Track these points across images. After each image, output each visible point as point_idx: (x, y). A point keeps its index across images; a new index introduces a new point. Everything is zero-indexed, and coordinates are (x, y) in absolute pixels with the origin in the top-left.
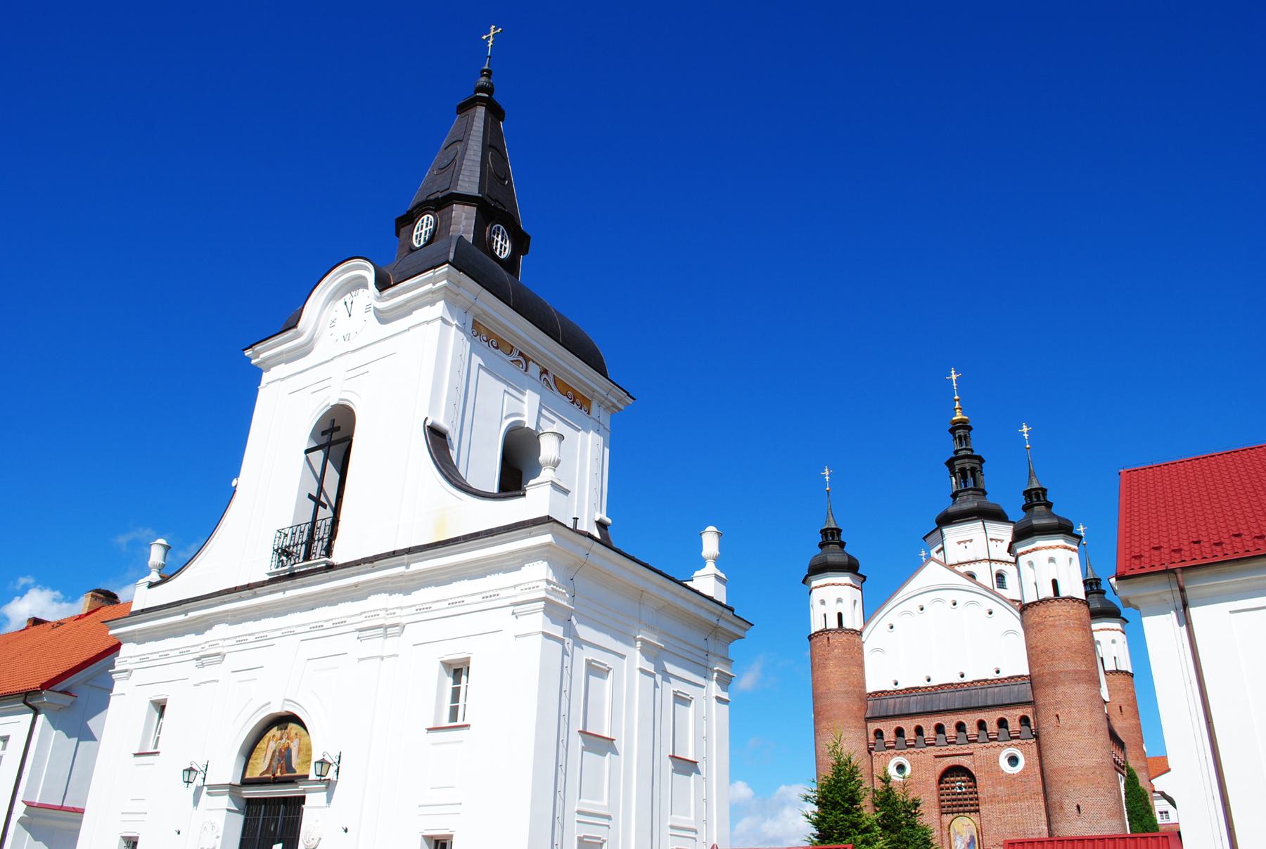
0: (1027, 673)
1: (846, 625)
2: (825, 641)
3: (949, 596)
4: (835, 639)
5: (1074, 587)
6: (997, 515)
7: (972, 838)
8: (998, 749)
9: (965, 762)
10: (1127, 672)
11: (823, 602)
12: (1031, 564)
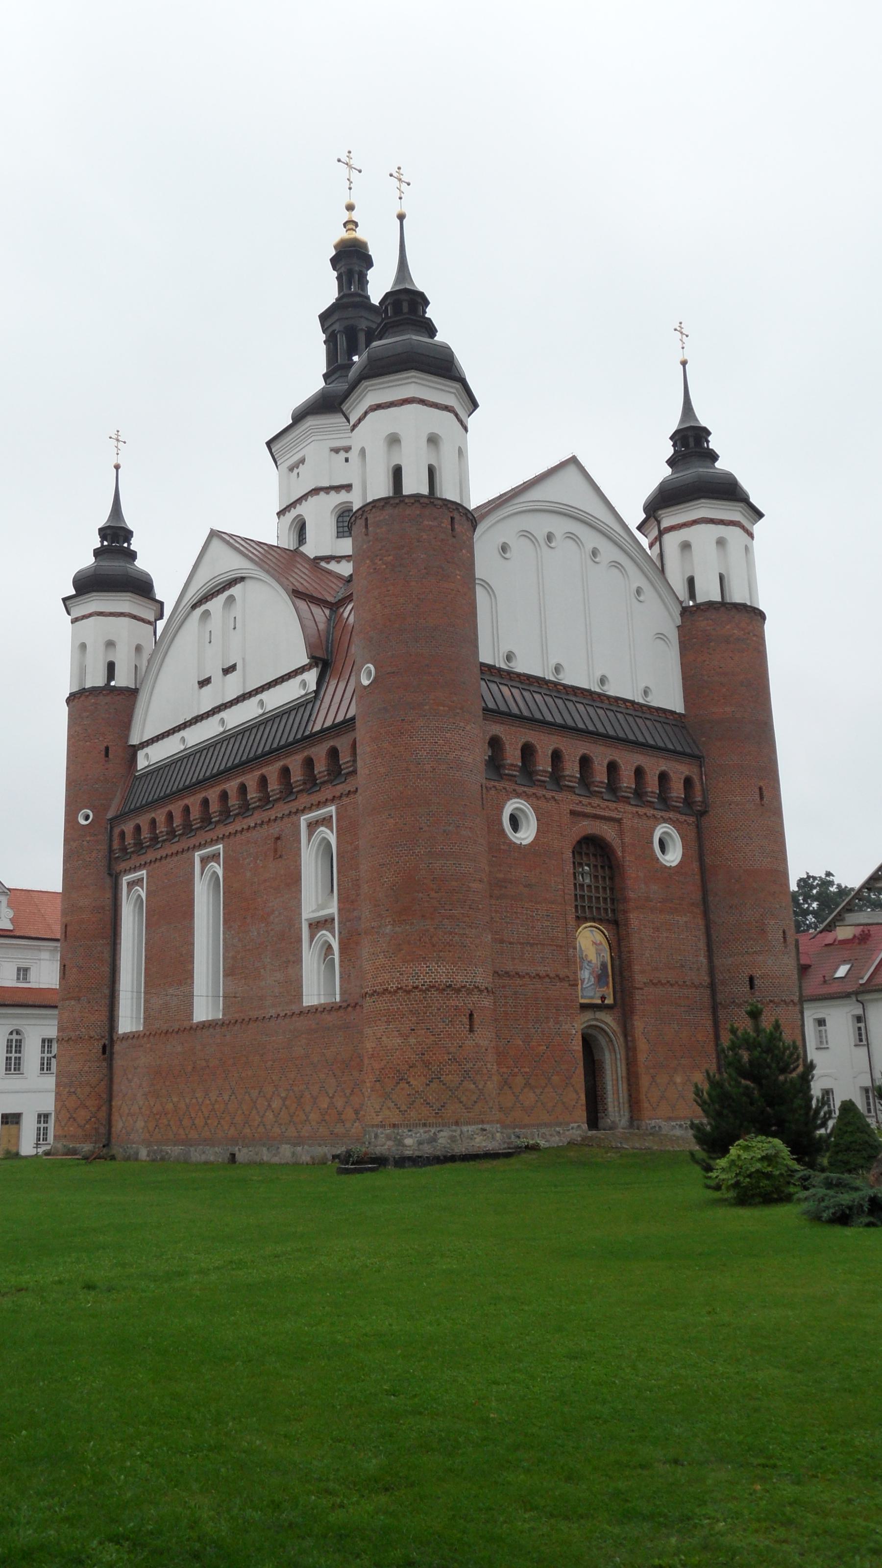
2: (446, 523)
3: (591, 539)
7: (604, 966)
9: (608, 832)
11: (433, 440)
12: (721, 542)
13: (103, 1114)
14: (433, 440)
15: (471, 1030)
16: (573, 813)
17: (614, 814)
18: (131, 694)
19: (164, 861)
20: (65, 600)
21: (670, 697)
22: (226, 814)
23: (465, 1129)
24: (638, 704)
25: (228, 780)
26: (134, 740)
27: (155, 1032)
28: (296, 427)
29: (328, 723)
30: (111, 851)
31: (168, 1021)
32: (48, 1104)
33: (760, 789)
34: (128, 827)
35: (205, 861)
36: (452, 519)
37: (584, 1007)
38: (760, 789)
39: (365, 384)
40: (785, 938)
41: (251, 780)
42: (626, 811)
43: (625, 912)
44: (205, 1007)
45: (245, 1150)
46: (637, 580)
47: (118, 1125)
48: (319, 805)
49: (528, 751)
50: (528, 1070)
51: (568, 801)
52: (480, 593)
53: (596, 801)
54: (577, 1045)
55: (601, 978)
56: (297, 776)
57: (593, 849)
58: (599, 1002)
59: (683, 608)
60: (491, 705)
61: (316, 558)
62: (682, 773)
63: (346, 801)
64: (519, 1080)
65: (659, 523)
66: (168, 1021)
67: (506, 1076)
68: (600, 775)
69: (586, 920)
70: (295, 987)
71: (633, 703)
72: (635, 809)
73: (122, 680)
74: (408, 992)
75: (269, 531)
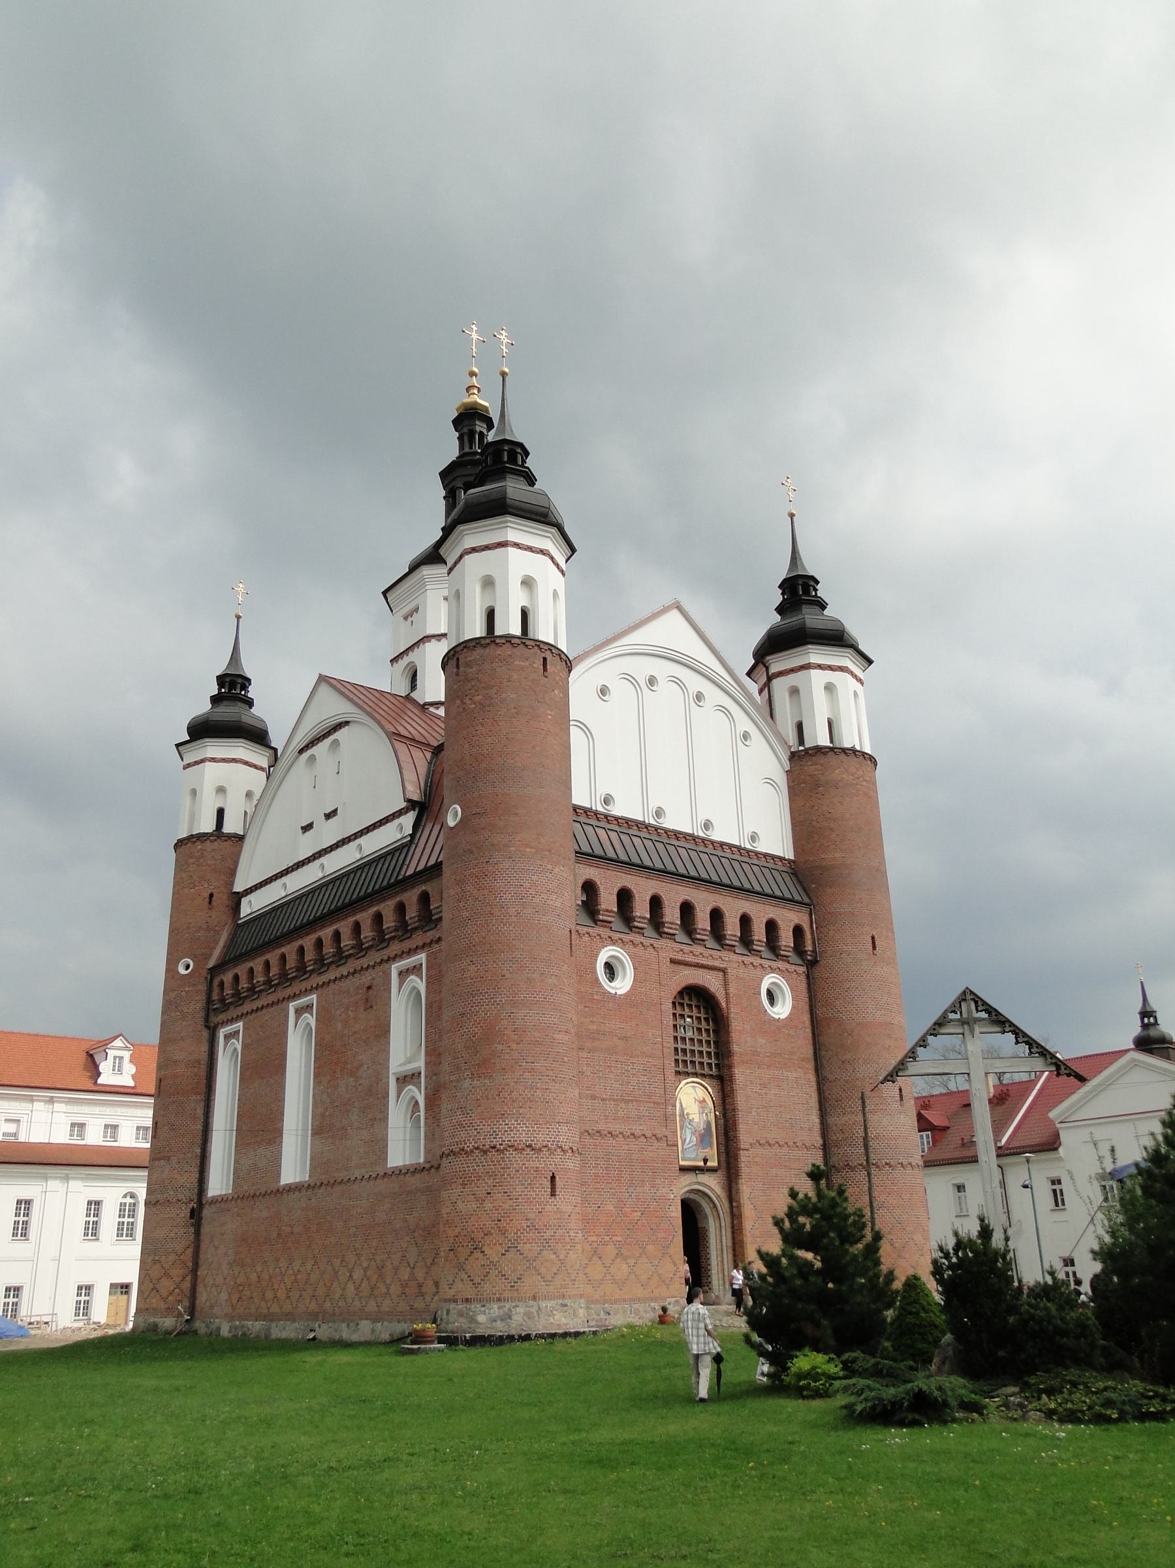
0: (790, 855)
2: (539, 664)
3: (696, 683)
8: (759, 971)
9: (712, 982)
12: (829, 688)
13: (187, 1285)
14: (528, 583)
15: (553, 1194)
16: (673, 961)
17: (717, 963)
18: (241, 838)
19: (259, 1013)
20: (177, 746)
21: (776, 840)
22: (322, 964)
23: (543, 1304)
24: (744, 849)
25: (323, 927)
26: (239, 887)
27: (241, 1197)
28: (412, 575)
29: (421, 867)
30: (209, 1001)
31: (258, 1186)
32: (131, 1273)
33: (873, 938)
34: (228, 978)
35: (299, 1012)
36: (545, 659)
37: (684, 1170)
38: (873, 938)
39: (461, 528)
40: (901, 1096)
41: (344, 927)
42: (732, 960)
43: (730, 1067)
44: (293, 1167)
45: (324, 1326)
46: (744, 724)
47: (202, 1297)
48: (410, 952)
49: (625, 897)
50: (620, 1239)
51: (668, 949)
52: (575, 734)
53: (698, 949)
54: (676, 1212)
55: (703, 1138)
56: (389, 922)
57: (697, 998)
58: (702, 1164)
59: (792, 753)
60: (586, 848)
61: (426, 704)
62: (791, 921)
63: (436, 948)
64: (611, 1250)
65: (767, 669)
66: (258, 1186)
67: (595, 1245)
68: (703, 922)
69: (688, 1074)
70: (380, 1146)
71: (739, 848)
72: (740, 958)
73: (231, 826)
74: (485, 1152)
75: (389, 681)
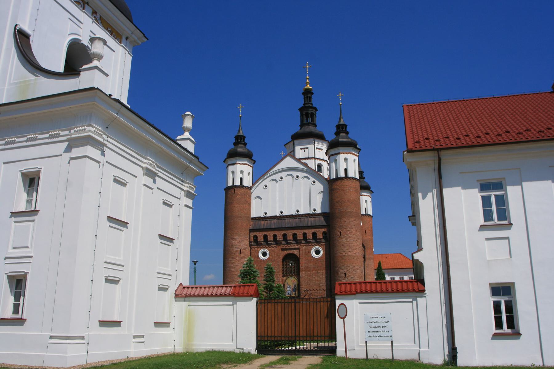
0: (327, 210)
1: (245, 184)
3: (295, 174)
4: (238, 191)
5: (354, 172)
6: (320, 137)
9: (296, 252)
10: (370, 215)
11: (233, 172)
17: (297, 247)
